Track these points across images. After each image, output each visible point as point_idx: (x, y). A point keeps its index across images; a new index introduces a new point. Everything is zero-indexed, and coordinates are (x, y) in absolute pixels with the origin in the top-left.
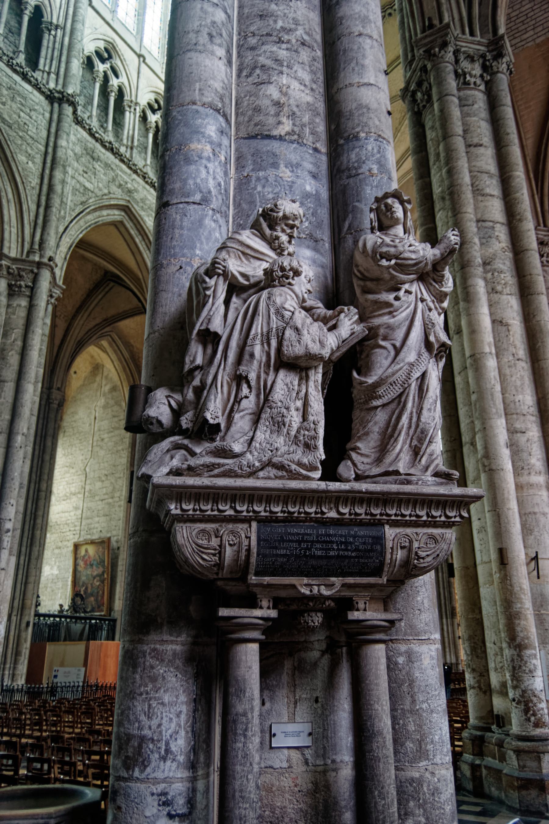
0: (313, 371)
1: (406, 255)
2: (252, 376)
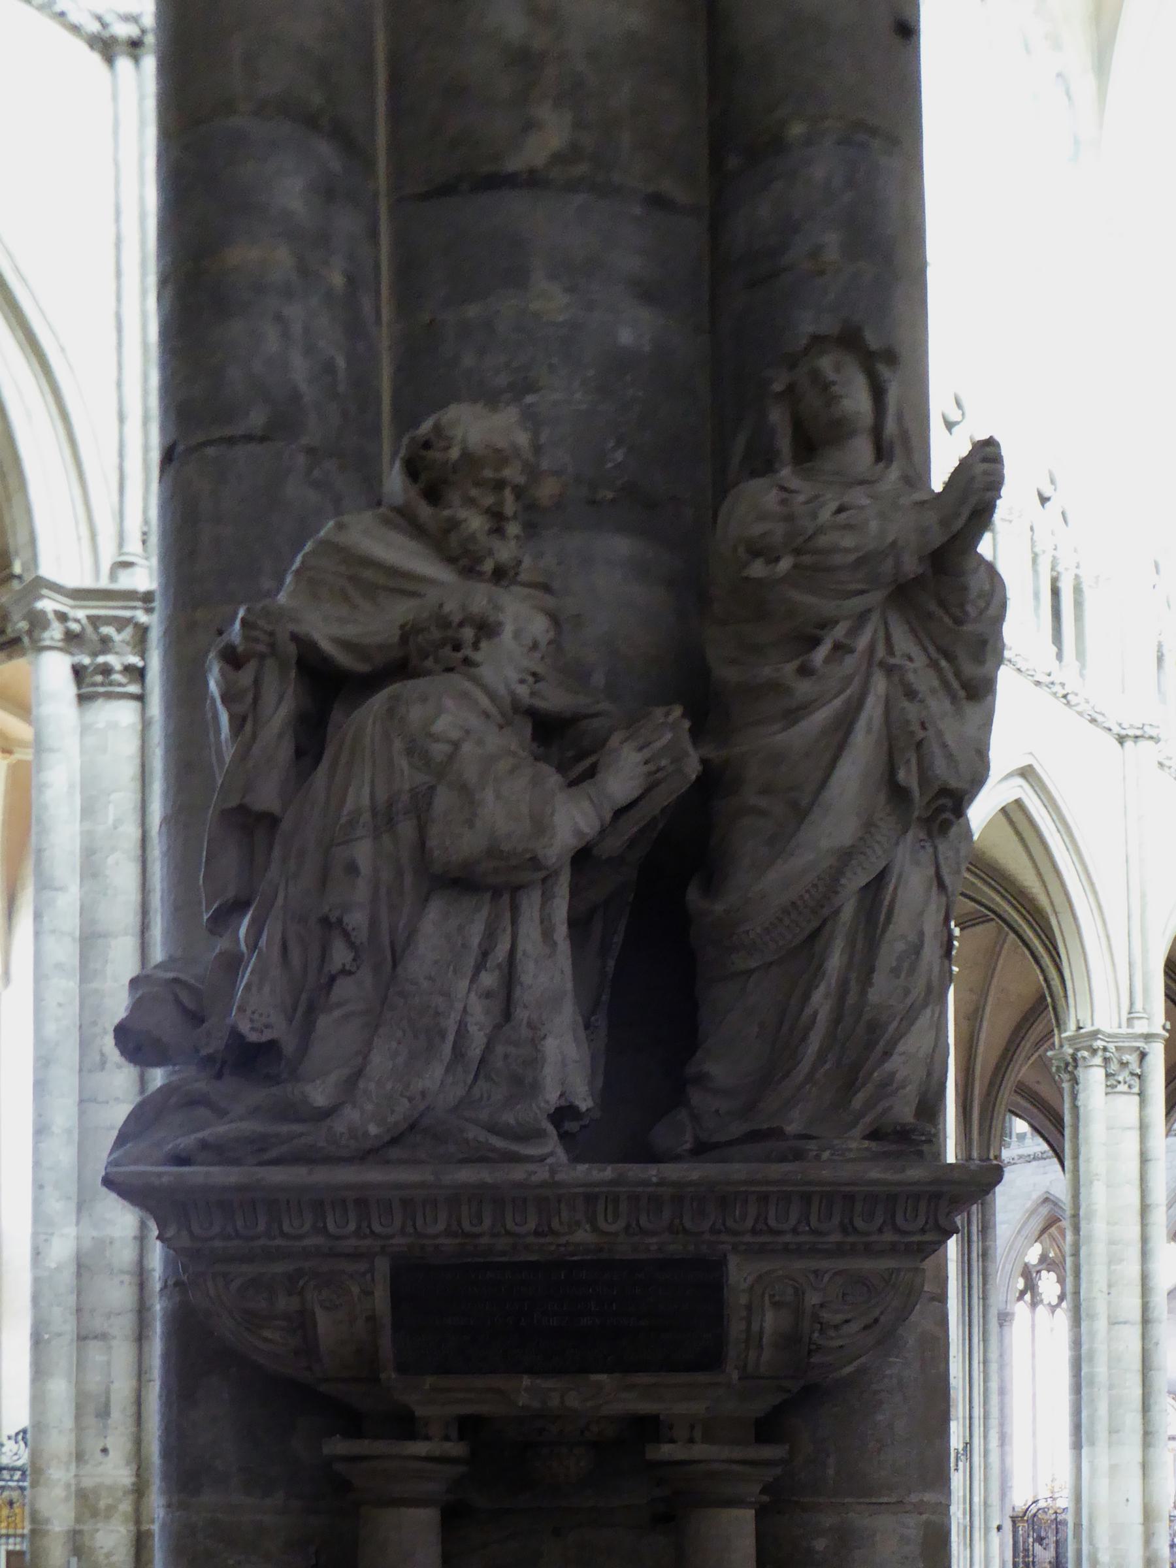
0: (536, 896)
1: (823, 541)
2: (357, 920)
